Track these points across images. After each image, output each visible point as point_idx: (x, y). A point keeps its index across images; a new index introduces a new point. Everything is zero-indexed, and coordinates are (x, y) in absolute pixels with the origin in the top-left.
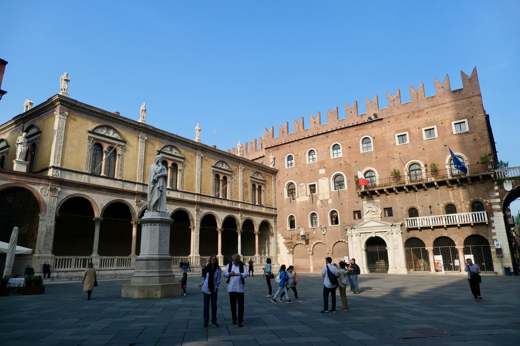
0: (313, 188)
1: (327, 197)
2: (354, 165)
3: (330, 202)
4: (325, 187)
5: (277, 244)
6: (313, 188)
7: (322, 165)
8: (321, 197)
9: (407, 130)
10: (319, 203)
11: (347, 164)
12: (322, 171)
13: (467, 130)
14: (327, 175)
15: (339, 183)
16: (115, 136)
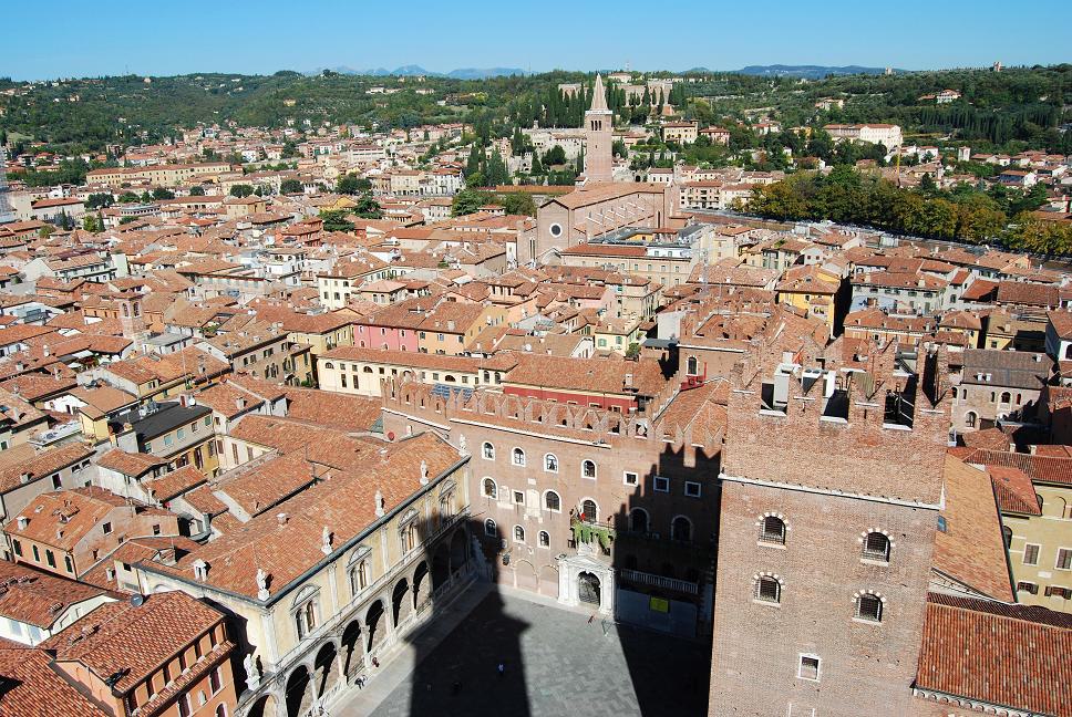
0: (519, 497)
1: (537, 514)
2: (571, 488)
3: (541, 521)
4: (535, 501)
5: (472, 545)
6: (519, 497)
7: (532, 473)
8: (528, 511)
9: (638, 471)
10: (526, 517)
11: (562, 484)
12: (532, 482)
13: (699, 495)
14: (539, 487)
15: (552, 501)
16: (311, 589)
